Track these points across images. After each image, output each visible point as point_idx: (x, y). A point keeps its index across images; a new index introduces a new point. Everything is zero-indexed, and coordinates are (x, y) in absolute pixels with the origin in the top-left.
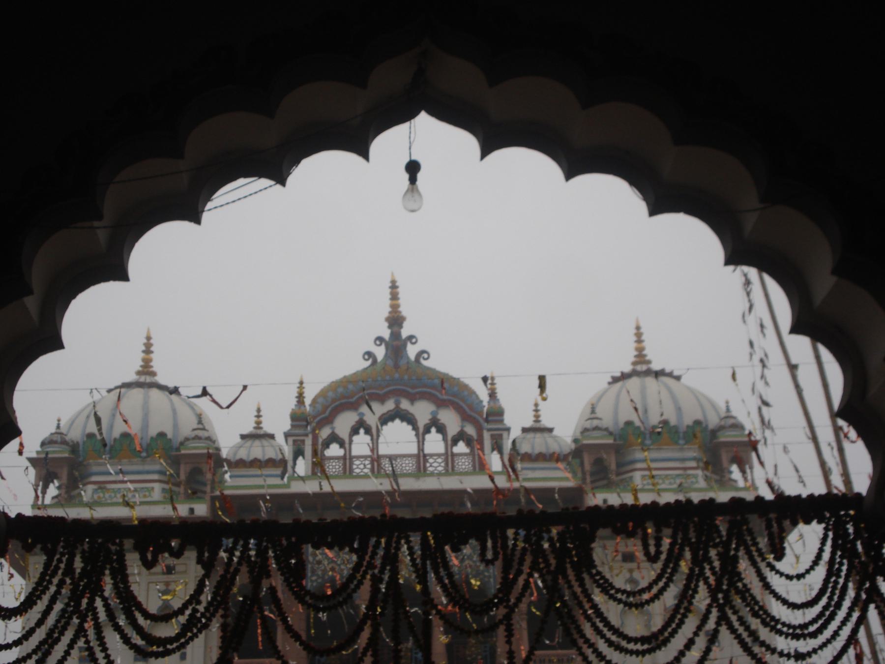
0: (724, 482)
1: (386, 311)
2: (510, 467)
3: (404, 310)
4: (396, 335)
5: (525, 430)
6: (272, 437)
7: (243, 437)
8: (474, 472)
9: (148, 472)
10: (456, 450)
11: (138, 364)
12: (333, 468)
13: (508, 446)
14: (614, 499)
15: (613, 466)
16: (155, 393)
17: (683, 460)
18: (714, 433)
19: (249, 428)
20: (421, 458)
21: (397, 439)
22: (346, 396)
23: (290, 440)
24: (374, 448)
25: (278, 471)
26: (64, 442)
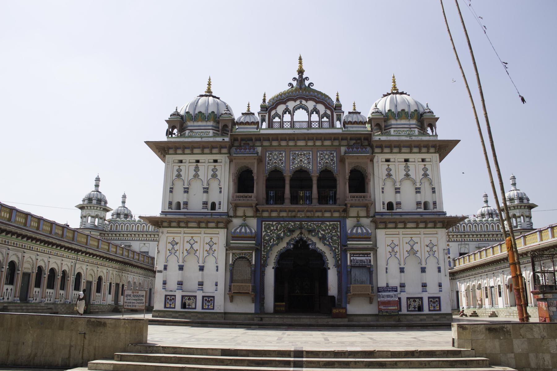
0: (425, 134)
1: (297, 67)
2: (345, 123)
3: (304, 68)
4: (301, 77)
5: (349, 113)
6: (253, 114)
7: (243, 114)
8: (330, 128)
9: (208, 126)
10: (323, 120)
11: (206, 89)
12: (276, 125)
13: (343, 118)
14: (383, 138)
15: (383, 127)
16: (211, 98)
17: (410, 124)
18: (422, 115)
19: (245, 111)
20: (310, 123)
21: (301, 116)
22: (281, 99)
23: (260, 115)
24: (292, 118)
25: (256, 126)
26: (178, 114)
